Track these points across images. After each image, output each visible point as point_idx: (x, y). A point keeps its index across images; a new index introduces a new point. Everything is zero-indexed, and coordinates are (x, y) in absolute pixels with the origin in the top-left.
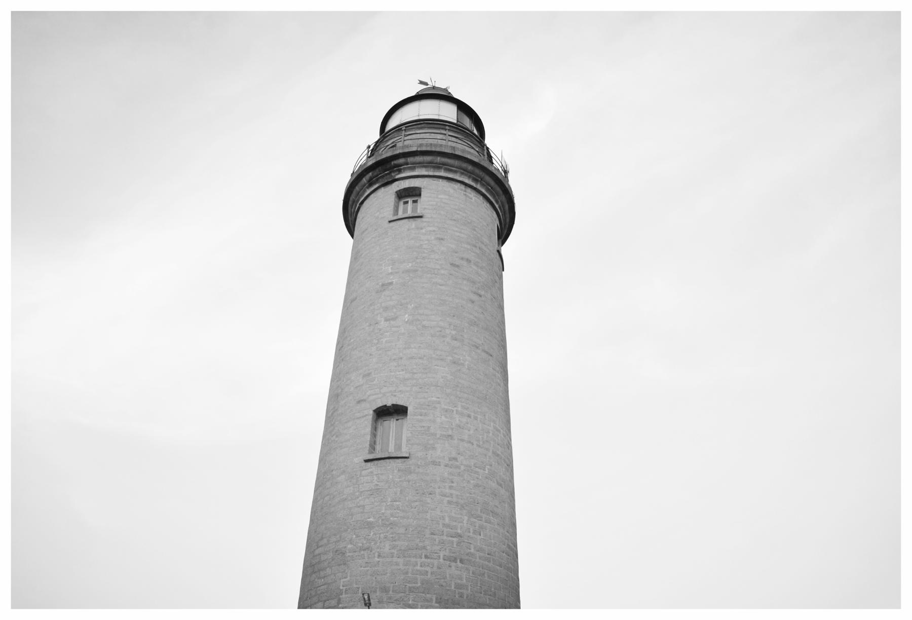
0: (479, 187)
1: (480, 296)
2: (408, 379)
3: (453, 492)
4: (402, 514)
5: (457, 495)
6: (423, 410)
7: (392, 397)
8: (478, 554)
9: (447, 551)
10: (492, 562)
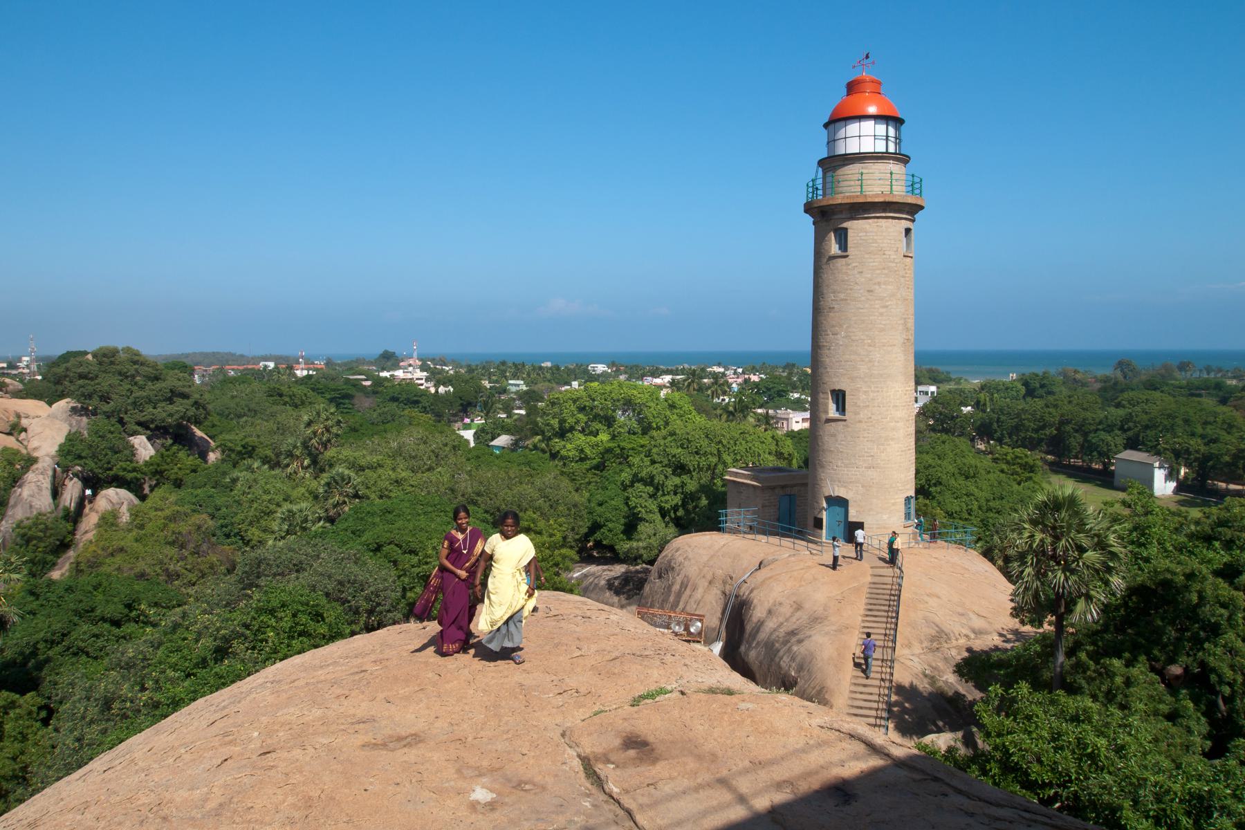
1: (887, 307)
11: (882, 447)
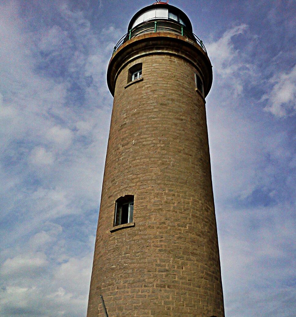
0: (180, 54)
1: (182, 120)
2: (133, 179)
3: (162, 243)
4: (130, 261)
5: (165, 245)
6: (143, 196)
7: (125, 191)
8: (181, 281)
9: (159, 281)
10: (192, 284)
11: (180, 261)
